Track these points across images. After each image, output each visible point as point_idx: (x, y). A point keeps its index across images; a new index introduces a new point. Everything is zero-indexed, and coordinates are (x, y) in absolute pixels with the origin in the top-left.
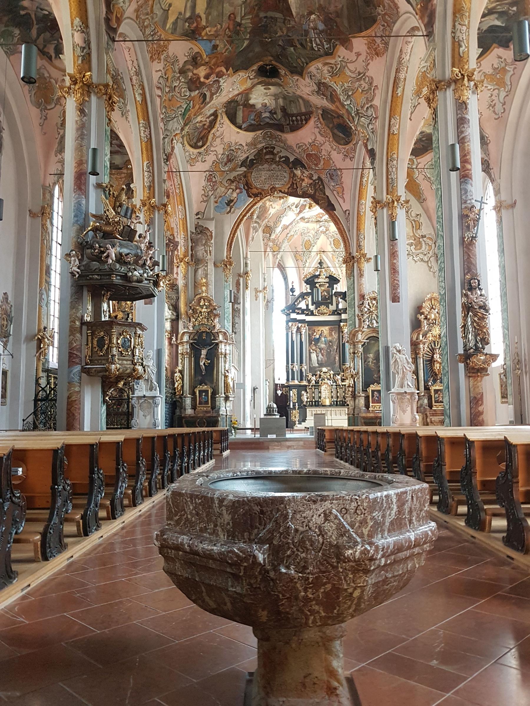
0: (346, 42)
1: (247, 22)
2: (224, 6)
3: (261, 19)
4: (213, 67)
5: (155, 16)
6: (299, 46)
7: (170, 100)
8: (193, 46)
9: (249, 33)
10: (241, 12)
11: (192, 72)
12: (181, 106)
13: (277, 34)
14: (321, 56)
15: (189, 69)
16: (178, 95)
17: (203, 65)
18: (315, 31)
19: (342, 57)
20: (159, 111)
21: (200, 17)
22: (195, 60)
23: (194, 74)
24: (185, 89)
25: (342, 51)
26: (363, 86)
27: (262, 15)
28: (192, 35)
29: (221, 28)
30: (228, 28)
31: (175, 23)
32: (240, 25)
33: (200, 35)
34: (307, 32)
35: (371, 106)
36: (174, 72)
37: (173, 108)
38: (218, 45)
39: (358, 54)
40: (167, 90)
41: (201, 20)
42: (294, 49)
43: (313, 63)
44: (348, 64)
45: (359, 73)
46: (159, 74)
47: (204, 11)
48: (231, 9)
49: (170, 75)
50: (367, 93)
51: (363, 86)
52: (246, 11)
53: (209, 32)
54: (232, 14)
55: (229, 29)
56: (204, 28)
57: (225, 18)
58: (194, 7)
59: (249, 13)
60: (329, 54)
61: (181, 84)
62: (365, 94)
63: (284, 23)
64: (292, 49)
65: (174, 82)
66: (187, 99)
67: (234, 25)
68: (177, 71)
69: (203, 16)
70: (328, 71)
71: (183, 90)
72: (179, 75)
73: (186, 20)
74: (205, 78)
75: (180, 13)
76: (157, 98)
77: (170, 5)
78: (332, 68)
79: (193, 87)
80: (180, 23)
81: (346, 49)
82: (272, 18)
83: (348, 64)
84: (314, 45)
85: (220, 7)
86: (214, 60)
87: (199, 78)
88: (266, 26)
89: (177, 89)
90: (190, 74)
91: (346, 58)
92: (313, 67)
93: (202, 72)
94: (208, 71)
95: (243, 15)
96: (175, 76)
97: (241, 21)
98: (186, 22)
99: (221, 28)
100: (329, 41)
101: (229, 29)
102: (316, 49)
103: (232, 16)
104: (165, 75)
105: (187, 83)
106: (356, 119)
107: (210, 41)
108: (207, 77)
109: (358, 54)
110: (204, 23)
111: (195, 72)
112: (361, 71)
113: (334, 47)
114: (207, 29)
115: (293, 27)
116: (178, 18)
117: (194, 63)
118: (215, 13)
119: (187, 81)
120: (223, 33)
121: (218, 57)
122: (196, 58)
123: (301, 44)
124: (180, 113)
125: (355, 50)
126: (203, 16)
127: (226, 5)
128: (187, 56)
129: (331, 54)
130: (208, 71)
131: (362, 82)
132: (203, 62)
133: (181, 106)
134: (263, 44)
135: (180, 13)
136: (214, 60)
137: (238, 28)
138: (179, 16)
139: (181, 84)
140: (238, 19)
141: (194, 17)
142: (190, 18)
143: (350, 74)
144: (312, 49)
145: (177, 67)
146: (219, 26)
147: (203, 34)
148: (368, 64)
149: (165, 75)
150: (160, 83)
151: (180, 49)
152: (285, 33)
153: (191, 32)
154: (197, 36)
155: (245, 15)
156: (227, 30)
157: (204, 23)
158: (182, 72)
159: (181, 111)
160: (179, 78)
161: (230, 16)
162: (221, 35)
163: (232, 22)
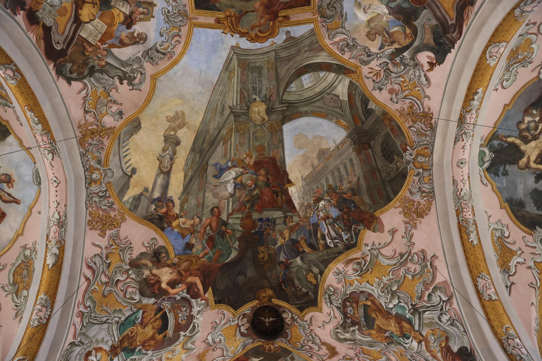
0: (371, 222)
1: (235, 222)
2: (206, 195)
3: (254, 222)
4: (183, 273)
5: (109, 174)
6: (307, 249)
7: (104, 296)
8: (157, 237)
9: (239, 240)
10: (227, 207)
11: (151, 271)
12: (120, 311)
13: (276, 244)
14: (340, 253)
15: (146, 265)
16: (121, 294)
17: (169, 266)
18: (327, 221)
19: (370, 245)
20: (80, 298)
21: (172, 202)
22: (157, 256)
23: (153, 275)
24: (134, 290)
25: (369, 237)
26: (412, 270)
27: (256, 216)
28: (160, 221)
29: (200, 222)
30: (210, 225)
31: (138, 199)
32: (225, 224)
33: (170, 224)
34: (316, 226)
35: (435, 289)
36: (123, 261)
37: (105, 308)
38: (193, 245)
39: (393, 232)
40: (104, 279)
41: (174, 206)
42: (302, 259)
43: (331, 265)
44: (382, 251)
45: (402, 255)
46: (98, 251)
47: (178, 196)
48: (215, 201)
49: (115, 261)
50: (421, 276)
51: (412, 270)
52: (235, 207)
53: (183, 223)
54: (216, 207)
55: (211, 226)
56: (177, 217)
57: (207, 211)
58: (165, 187)
59: (239, 210)
60: (350, 246)
61: (129, 280)
62: (419, 278)
63: (285, 223)
64: (298, 260)
65: (119, 275)
66: (134, 304)
67: (218, 223)
68: (128, 261)
69: (177, 202)
70: (356, 270)
71: (130, 290)
72: (128, 267)
73: (153, 201)
74: (168, 284)
75: (146, 190)
76: (83, 279)
77: (134, 171)
78: (359, 264)
79: (148, 292)
80: (144, 202)
81: (374, 231)
82: (268, 220)
83: (382, 251)
84: (328, 241)
85: (201, 196)
86: (186, 264)
87: (159, 282)
88: (260, 234)
89: (120, 285)
90: (147, 273)
91: (377, 243)
92: (331, 274)
93: (166, 275)
94: (174, 276)
95: (230, 211)
96: (121, 267)
97: (227, 220)
98: (152, 203)
99: (200, 222)
100: (348, 229)
101: (211, 226)
102: (332, 245)
103: (215, 211)
104: (107, 258)
105: (140, 283)
106: (416, 322)
107: (183, 237)
108: (173, 284)
109: (393, 232)
110: (177, 210)
111: (155, 271)
112: (404, 251)
113: (357, 235)
114: (182, 220)
115: (298, 224)
116: (142, 194)
117: (155, 259)
118: (193, 202)
119: (139, 279)
120: (202, 231)
121: (192, 262)
122: (160, 254)
123: (311, 246)
124: (117, 319)
125: (387, 228)
126: (177, 202)
127: (209, 195)
128: (147, 247)
129: (355, 245)
130: (174, 276)
131: (409, 265)
132: (169, 262)
133: (120, 311)
134: (258, 265)
135: (146, 190)
136: (186, 264)
137: (223, 228)
138: (144, 193)
139: (129, 282)
140: (224, 217)
141: (164, 200)
142: (159, 200)
143: (387, 262)
144: (327, 247)
145: (129, 256)
146: (197, 220)
147: (174, 224)
148: (411, 236)
149: (107, 258)
150: (95, 263)
151: (139, 236)
152: (287, 236)
153: (157, 217)
154: (165, 225)
155: (233, 211)
156: (208, 228)
157: (177, 210)
158: (135, 264)
159: (120, 318)
160: (127, 271)
161: (212, 209)
162: (200, 232)
163: (215, 218)
